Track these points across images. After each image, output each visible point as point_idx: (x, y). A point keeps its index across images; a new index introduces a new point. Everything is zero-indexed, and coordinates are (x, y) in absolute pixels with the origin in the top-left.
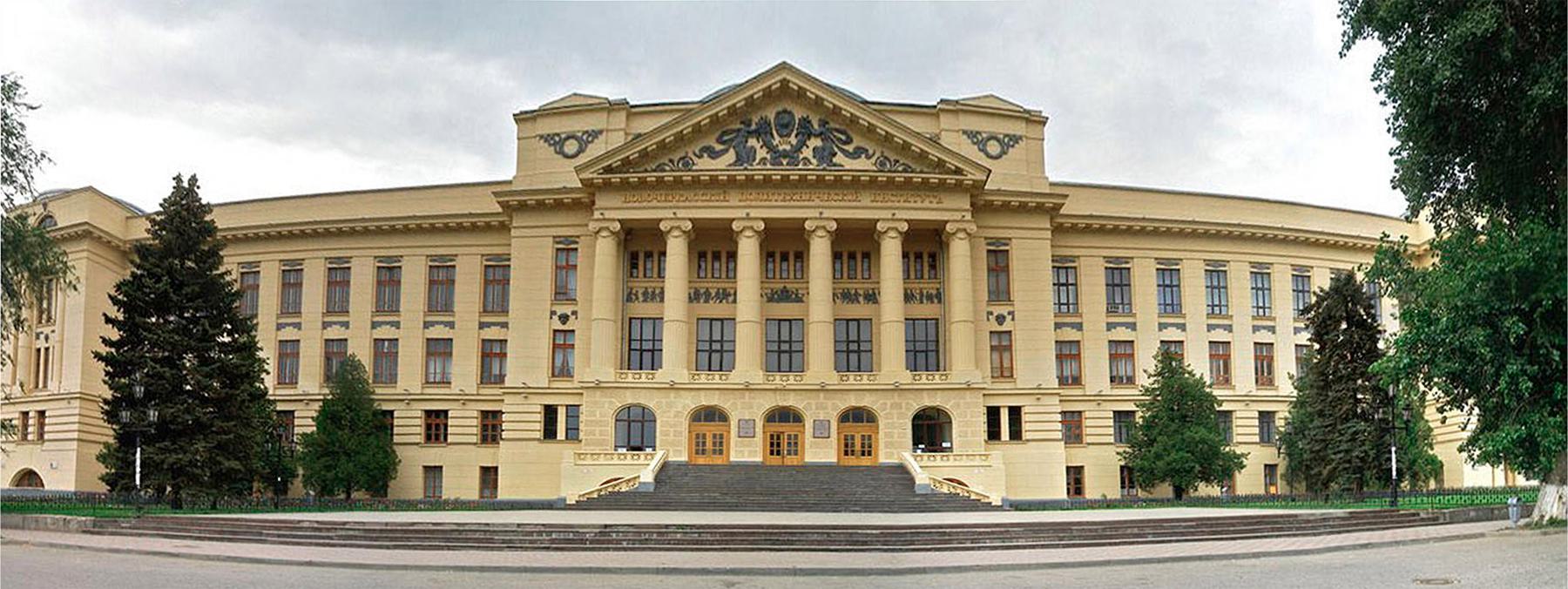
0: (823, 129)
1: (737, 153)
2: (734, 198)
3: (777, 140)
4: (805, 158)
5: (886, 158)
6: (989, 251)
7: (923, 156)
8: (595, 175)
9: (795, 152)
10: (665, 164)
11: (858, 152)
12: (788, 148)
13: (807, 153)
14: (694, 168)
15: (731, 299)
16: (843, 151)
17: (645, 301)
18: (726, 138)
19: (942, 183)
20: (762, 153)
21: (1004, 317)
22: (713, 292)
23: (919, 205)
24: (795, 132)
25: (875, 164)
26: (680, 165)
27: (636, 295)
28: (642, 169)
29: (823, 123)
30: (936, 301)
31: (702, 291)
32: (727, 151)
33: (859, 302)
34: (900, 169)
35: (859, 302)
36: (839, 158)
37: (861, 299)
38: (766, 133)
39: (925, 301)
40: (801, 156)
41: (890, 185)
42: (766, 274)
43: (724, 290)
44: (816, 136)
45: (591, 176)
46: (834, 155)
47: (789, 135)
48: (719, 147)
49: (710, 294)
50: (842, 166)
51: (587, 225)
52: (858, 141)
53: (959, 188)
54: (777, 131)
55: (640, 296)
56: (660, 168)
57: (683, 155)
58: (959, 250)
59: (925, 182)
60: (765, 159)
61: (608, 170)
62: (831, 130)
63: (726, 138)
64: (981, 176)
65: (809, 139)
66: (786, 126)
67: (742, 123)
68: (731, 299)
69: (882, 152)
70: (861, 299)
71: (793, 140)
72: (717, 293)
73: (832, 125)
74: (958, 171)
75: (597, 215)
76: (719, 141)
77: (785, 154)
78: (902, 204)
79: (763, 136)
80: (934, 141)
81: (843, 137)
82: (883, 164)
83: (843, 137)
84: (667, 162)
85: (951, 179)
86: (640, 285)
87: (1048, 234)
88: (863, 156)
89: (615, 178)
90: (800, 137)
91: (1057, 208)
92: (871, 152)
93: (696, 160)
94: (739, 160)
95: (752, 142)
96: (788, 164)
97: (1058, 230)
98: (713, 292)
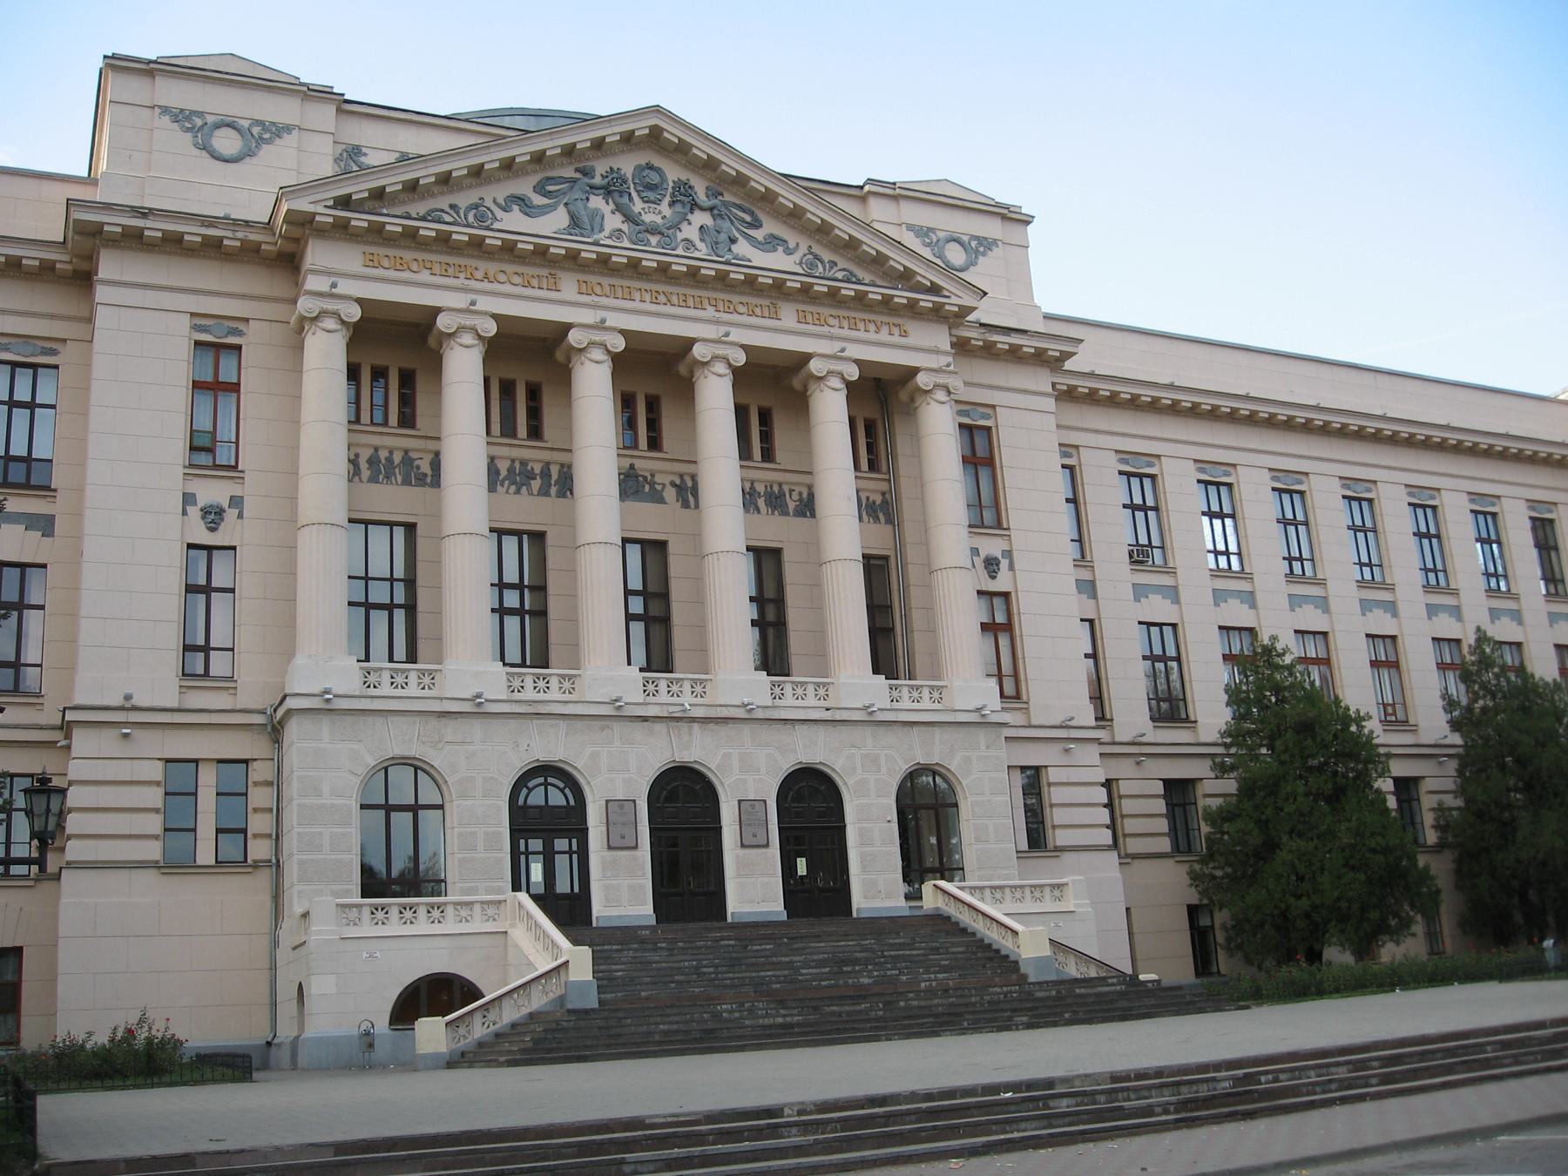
0: (714, 202)
1: (569, 212)
2: (569, 285)
3: (638, 206)
5: (816, 257)
8: (320, 209)
10: (442, 211)
11: (772, 243)
12: (659, 220)
13: (690, 232)
14: (496, 225)
15: (536, 484)
16: (748, 237)
17: (373, 479)
19: (912, 306)
20: (614, 222)
22: (503, 467)
23: (872, 336)
25: (800, 263)
26: (471, 219)
28: (398, 211)
29: (713, 193)
30: (881, 516)
32: (553, 207)
34: (840, 275)
36: (742, 248)
37: (761, 503)
40: (680, 236)
41: (833, 297)
43: (524, 463)
44: (702, 209)
45: (311, 208)
46: (733, 241)
47: (658, 202)
48: (539, 200)
49: (498, 473)
51: (295, 302)
52: (770, 227)
53: (937, 315)
57: (475, 200)
59: (887, 301)
60: (620, 230)
61: (344, 202)
62: (726, 204)
64: (967, 300)
65: (692, 213)
66: (651, 187)
67: (577, 170)
68: (536, 484)
70: (761, 503)
71: (664, 207)
72: (511, 470)
73: (728, 197)
74: (934, 289)
75: (313, 283)
76: (540, 189)
77: (653, 230)
78: (846, 332)
79: (616, 195)
81: (748, 218)
82: (812, 266)
83: (748, 218)
84: (448, 209)
85: (927, 301)
88: (780, 249)
89: (359, 221)
90: (678, 207)
92: (792, 245)
93: (499, 213)
94: (575, 222)
95: (597, 202)
96: (659, 244)
98: (503, 467)
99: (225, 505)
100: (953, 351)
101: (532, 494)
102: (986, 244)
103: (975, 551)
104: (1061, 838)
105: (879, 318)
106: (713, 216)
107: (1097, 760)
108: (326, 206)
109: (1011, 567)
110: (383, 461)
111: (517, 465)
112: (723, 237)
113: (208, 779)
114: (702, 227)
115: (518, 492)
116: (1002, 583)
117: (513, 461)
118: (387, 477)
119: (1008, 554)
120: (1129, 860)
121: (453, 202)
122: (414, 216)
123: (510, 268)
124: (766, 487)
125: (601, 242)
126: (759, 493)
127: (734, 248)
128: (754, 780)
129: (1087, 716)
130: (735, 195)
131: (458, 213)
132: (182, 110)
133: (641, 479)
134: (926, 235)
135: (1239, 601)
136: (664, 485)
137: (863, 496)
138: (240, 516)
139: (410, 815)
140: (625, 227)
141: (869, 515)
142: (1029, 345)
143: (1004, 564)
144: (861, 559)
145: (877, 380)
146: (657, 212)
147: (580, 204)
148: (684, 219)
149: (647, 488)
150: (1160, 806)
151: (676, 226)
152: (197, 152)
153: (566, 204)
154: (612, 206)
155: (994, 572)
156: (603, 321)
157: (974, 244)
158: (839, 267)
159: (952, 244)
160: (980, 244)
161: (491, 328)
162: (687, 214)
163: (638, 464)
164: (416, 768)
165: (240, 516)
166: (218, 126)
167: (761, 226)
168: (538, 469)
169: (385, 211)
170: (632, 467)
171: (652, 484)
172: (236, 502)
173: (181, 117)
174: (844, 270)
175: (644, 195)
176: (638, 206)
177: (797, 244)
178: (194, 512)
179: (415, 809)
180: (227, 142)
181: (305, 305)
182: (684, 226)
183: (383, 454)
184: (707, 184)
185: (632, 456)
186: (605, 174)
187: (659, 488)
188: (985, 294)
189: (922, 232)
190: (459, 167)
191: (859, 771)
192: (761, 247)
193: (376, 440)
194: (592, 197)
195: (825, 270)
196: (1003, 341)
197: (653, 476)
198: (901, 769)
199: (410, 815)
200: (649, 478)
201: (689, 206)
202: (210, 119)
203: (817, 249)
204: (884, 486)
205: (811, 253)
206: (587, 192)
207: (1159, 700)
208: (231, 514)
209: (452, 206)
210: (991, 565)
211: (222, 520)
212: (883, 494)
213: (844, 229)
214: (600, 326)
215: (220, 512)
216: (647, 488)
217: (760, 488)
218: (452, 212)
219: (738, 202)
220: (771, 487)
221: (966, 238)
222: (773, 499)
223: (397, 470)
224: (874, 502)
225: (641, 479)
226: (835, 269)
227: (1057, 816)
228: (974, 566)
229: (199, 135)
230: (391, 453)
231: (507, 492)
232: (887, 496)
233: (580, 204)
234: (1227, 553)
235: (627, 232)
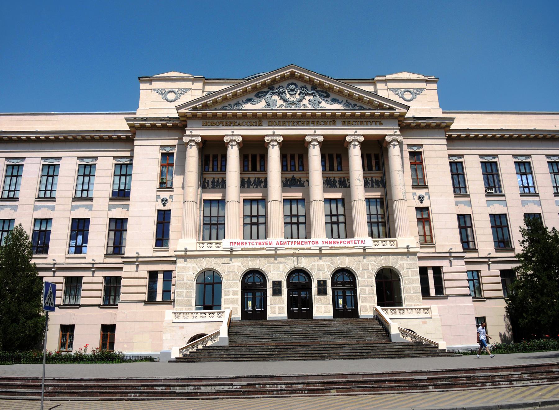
1: (266, 102)
4: (304, 105)
6: (410, 153)
7: (370, 102)
8: (187, 111)
9: (298, 102)
10: (227, 107)
12: (295, 100)
15: (262, 185)
18: (260, 95)
20: (280, 102)
21: (423, 197)
22: (252, 180)
24: (298, 93)
27: (208, 183)
30: (381, 185)
31: (246, 180)
33: (336, 187)
34: (357, 108)
35: (336, 187)
37: (337, 184)
38: (282, 93)
39: (374, 185)
42: (284, 168)
43: (259, 179)
46: (320, 103)
49: (251, 182)
50: (325, 108)
51: (182, 139)
54: (288, 92)
55: (210, 183)
56: (224, 108)
58: (394, 152)
60: (282, 105)
61: (195, 109)
63: (260, 95)
64: (403, 110)
67: (268, 89)
68: (262, 185)
69: (347, 101)
70: (337, 184)
71: (297, 96)
72: (255, 181)
74: (391, 108)
75: (188, 133)
77: (293, 103)
80: (376, 95)
83: (325, 95)
84: (228, 106)
85: (387, 113)
86: (210, 177)
87: (445, 141)
89: (199, 113)
90: (301, 95)
91: (448, 126)
92: (340, 101)
94: (268, 104)
95: (275, 97)
97: (450, 139)
98: (252, 180)
99: (168, 198)
100: (399, 128)
101: (261, 188)
102: (419, 91)
103: (415, 194)
104: (447, 292)
105: (372, 120)
106: (313, 96)
107: (464, 264)
108: (189, 110)
109: (429, 198)
110: (216, 182)
111: (257, 179)
112: (316, 101)
113: (160, 277)
114: (309, 100)
115: (257, 187)
116: (425, 204)
117: (255, 178)
118: (217, 186)
119: (428, 194)
120: (485, 299)
121: (230, 103)
122: (218, 109)
123: (246, 121)
124: (339, 179)
125: (274, 109)
126: (337, 181)
127: (320, 105)
128: (323, 273)
129: (458, 247)
130: (321, 88)
131: (231, 107)
132: (159, 89)
133: (296, 180)
134: (396, 91)
135: (537, 205)
136: (304, 181)
137: (374, 179)
138: (172, 201)
139: (211, 286)
140: (284, 104)
141: (376, 185)
142: (433, 123)
143: (426, 197)
144: (365, 200)
145: (378, 141)
147: (269, 98)
148: (304, 98)
149: (298, 183)
150: (499, 279)
151: (301, 101)
152: (163, 100)
153: (265, 99)
155: (422, 200)
156: (274, 132)
157: (415, 91)
158: (358, 105)
159: (406, 93)
160: (417, 91)
161: (281, 139)
163: (295, 176)
164: (214, 272)
165: (172, 201)
166: (169, 92)
167: (330, 96)
168: (263, 180)
169: (208, 109)
170: (293, 176)
171: (300, 181)
172: (171, 197)
173: (158, 91)
174: (359, 106)
176: (288, 96)
177: (343, 100)
178: (160, 201)
179: (213, 284)
180: (171, 96)
181: (185, 139)
182: (304, 100)
183: (216, 180)
184: (311, 86)
185: (293, 173)
187: (302, 182)
188: (409, 107)
189: (395, 90)
190: (229, 94)
191: (361, 269)
193: (213, 176)
194: (273, 96)
195: (352, 107)
196: (423, 123)
197: (300, 178)
198: (377, 268)
199: (211, 286)
200: (299, 179)
201: (304, 95)
202: (167, 90)
203: (349, 101)
204: (381, 175)
205: (347, 102)
206: (271, 95)
207: (499, 242)
208: (170, 201)
209: (229, 105)
210: (421, 198)
211: (167, 202)
212: (381, 177)
213: (357, 94)
214: (274, 135)
215: (166, 200)
216: (298, 183)
217: (337, 179)
218: (229, 107)
219: (322, 90)
220: (341, 179)
221: (412, 90)
222: (341, 182)
223: (220, 184)
224: (378, 180)
225: (296, 180)
226: (356, 106)
227: (446, 284)
228: (414, 199)
229: (164, 95)
230: (218, 179)
231: (253, 188)
232: (383, 178)
233: (269, 98)
234: (528, 187)
235: (284, 105)
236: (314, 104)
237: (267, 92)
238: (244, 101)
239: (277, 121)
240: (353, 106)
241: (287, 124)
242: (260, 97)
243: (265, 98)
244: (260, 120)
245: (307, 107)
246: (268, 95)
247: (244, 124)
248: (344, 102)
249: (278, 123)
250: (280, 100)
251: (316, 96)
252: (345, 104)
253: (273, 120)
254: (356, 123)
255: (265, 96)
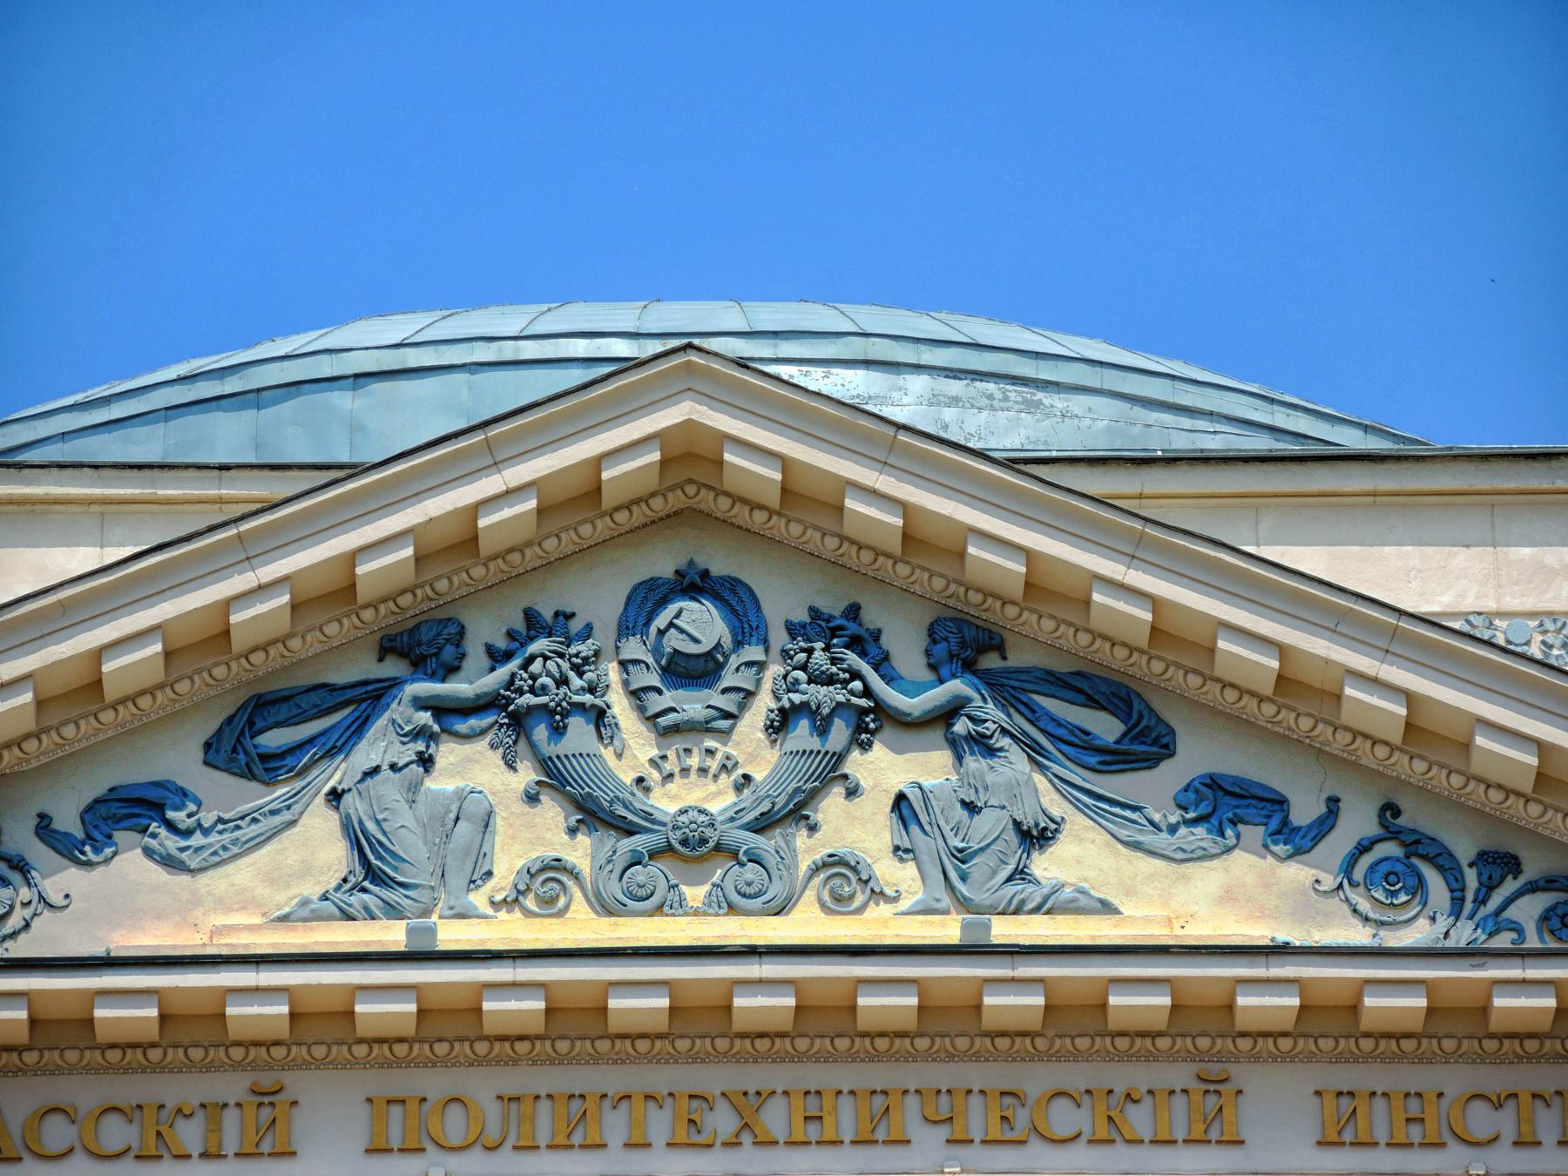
4: (834, 862)
9: (762, 825)
12: (718, 799)
18: (274, 739)
46: (1036, 837)
54: (636, 694)
60: (557, 865)
63: (274, 739)
65: (866, 747)
83: (1106, 727)
90: (802, 735)
92: (1304, 811)
106: (955, 745)
112: (989, 825)
114: (901, 798)
127: (1044, 866)
140: (580, 852)
146: (714, 764)
153: (335, 796)
154: (527, 774)
158: (1530, 871)
162: (840, 758)
175: (656, 703)
177: (1333, 802)
182: (831, 807)
186: (502, 644)
192: (1161, 840)
194: (448, 753)
201: (840, 732)
205: (1391, 833)
226: (1510, 886)
233: (388, 788)
236: (962, 856)
237: (374, 695)
238: (68, 821)
239: (484, 1086)
240: (1471, 878)
241: (615, 1125)
242: (268, 768)
243: (337, 773)
244: (266, 1080)
245: (878, 895)
246: (377, 747)
247: (57, 1133)
248: (1357, 821)
249: (493, 1113)
250: (532, 798)
251: (991, 752)
252: (1363, 848)
253: (436, 1084)
254: (1505, 1121)
255: (337, 746)
